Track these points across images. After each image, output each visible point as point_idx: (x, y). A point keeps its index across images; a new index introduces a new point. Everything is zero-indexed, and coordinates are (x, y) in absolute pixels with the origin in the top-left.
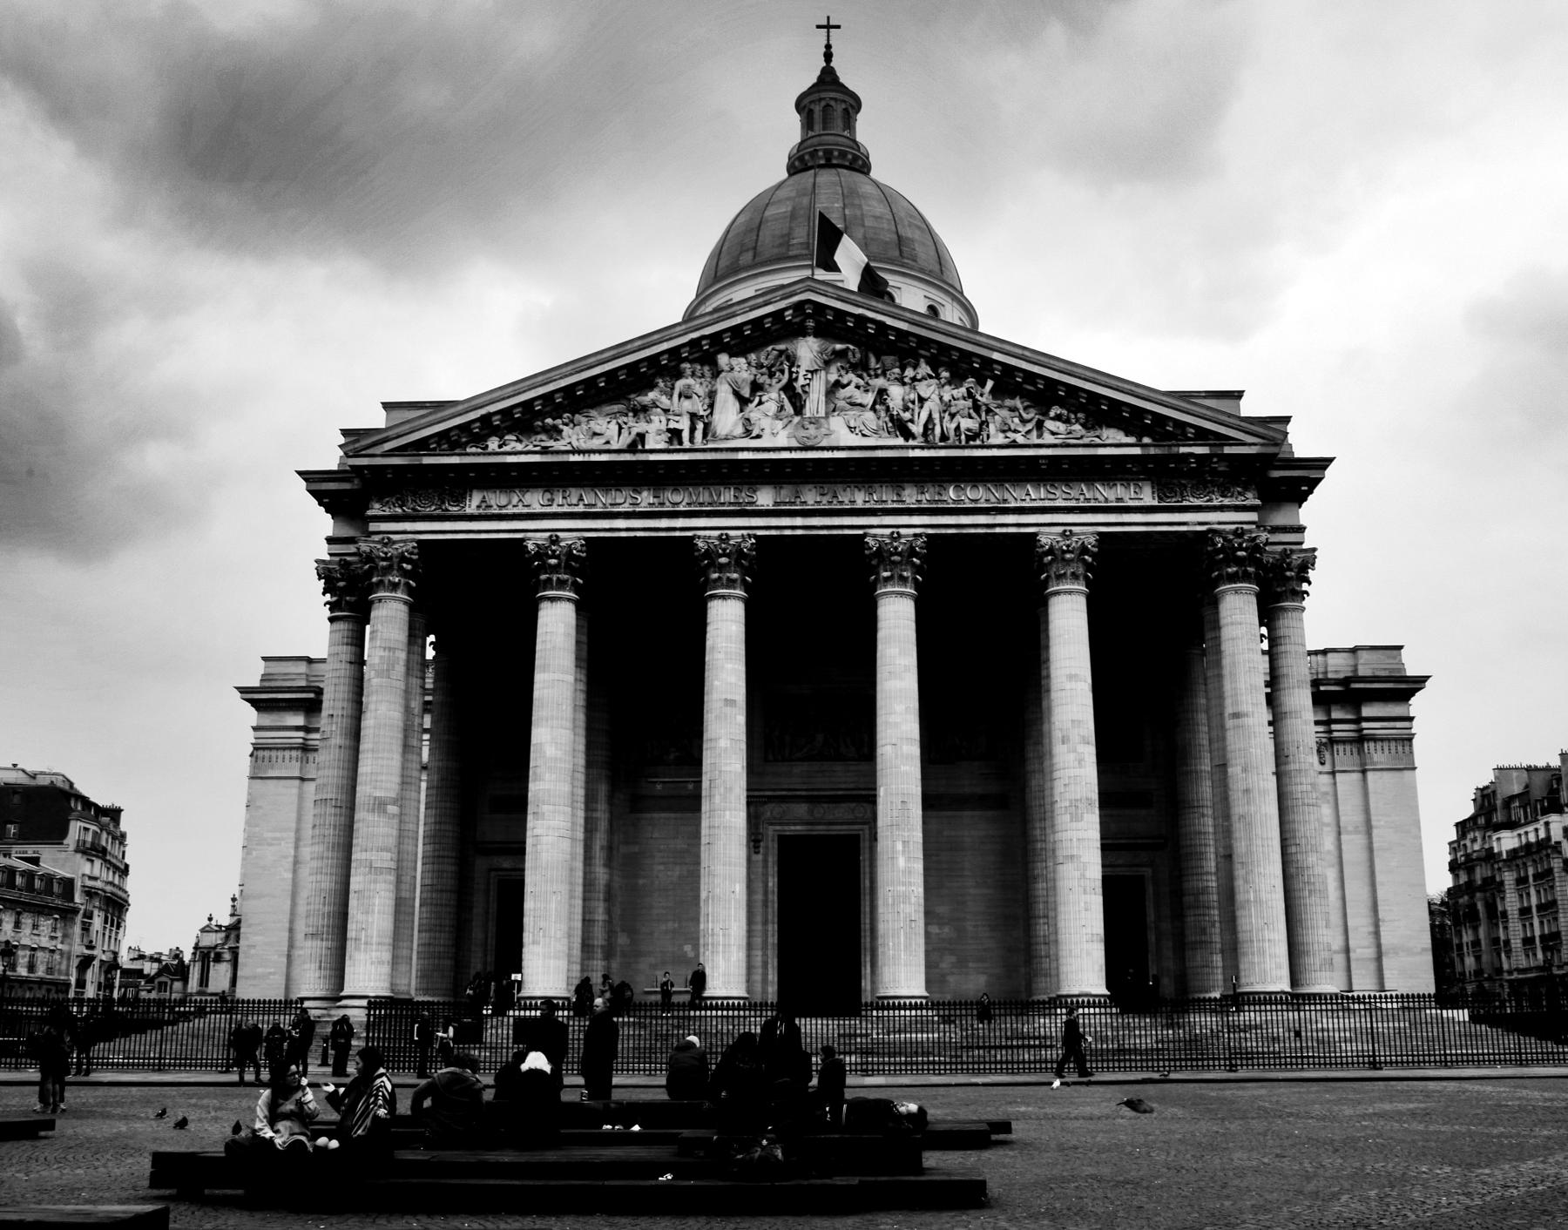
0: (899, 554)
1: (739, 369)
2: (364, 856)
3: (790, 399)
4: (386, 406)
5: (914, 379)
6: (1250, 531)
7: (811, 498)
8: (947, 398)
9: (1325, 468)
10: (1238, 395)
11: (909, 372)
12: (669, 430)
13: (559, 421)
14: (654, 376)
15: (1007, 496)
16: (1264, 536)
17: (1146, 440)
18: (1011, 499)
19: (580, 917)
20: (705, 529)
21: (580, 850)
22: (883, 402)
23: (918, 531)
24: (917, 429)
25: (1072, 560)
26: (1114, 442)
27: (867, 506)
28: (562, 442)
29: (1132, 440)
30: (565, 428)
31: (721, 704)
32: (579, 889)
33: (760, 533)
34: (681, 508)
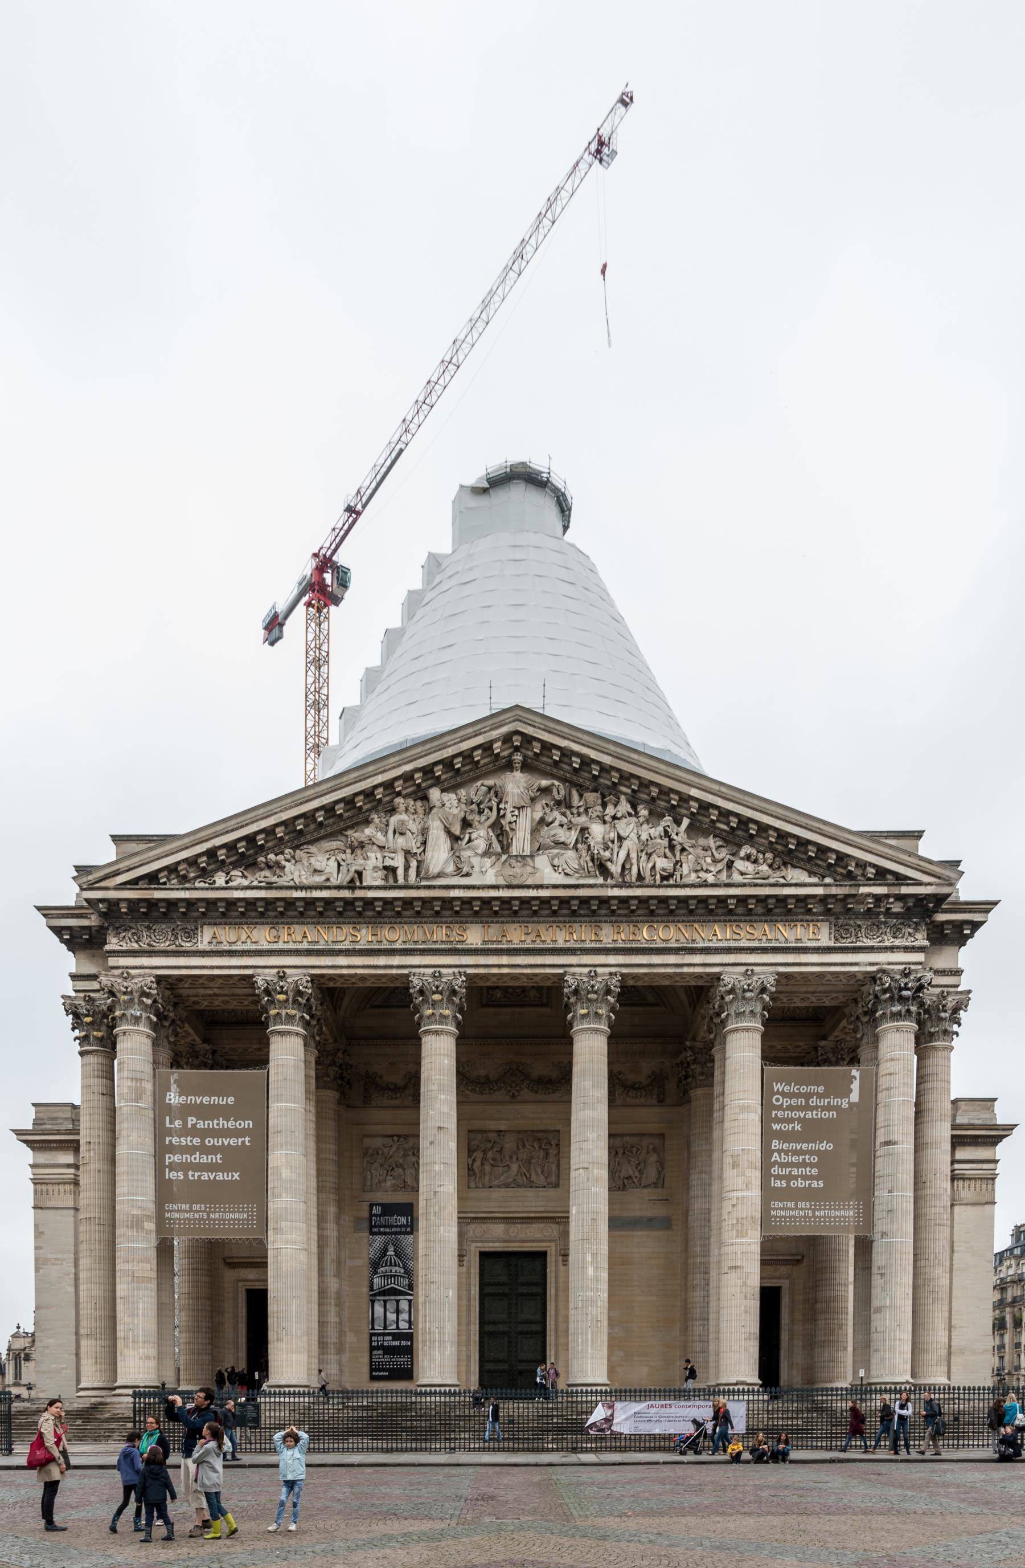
0: (596, 992)
1: (450, 804)
2: (126, 1266)
3: (498, 836)
4: (117, 839)
5: (614, 818)
6: (916, 971)
7: (516, 935)
8: (644, 837)
9: (988, 911)
10: (918, 835)
11: (610, 810)
12: (385, 868)
13: (280, 857)
14: (369, 810)
15: (696, 936)
16: (929, 975)
17: (828, 880)
18: (699, 939)
19: (316, 1319)
20: (420, 969)
21: (315, 1262)
22: (585, 840)
23: (613, 970)
24: (615, 869)
25: (751, 999)
26: (799, 882)
27: (568, 945)
28: (285, 878)
29: (814, 880)
30: (287, 864)
31: (435, 1131)
32: (316, 1295)
33: (469, 971)
34: (397, 946)
